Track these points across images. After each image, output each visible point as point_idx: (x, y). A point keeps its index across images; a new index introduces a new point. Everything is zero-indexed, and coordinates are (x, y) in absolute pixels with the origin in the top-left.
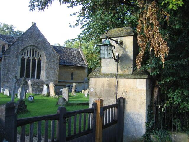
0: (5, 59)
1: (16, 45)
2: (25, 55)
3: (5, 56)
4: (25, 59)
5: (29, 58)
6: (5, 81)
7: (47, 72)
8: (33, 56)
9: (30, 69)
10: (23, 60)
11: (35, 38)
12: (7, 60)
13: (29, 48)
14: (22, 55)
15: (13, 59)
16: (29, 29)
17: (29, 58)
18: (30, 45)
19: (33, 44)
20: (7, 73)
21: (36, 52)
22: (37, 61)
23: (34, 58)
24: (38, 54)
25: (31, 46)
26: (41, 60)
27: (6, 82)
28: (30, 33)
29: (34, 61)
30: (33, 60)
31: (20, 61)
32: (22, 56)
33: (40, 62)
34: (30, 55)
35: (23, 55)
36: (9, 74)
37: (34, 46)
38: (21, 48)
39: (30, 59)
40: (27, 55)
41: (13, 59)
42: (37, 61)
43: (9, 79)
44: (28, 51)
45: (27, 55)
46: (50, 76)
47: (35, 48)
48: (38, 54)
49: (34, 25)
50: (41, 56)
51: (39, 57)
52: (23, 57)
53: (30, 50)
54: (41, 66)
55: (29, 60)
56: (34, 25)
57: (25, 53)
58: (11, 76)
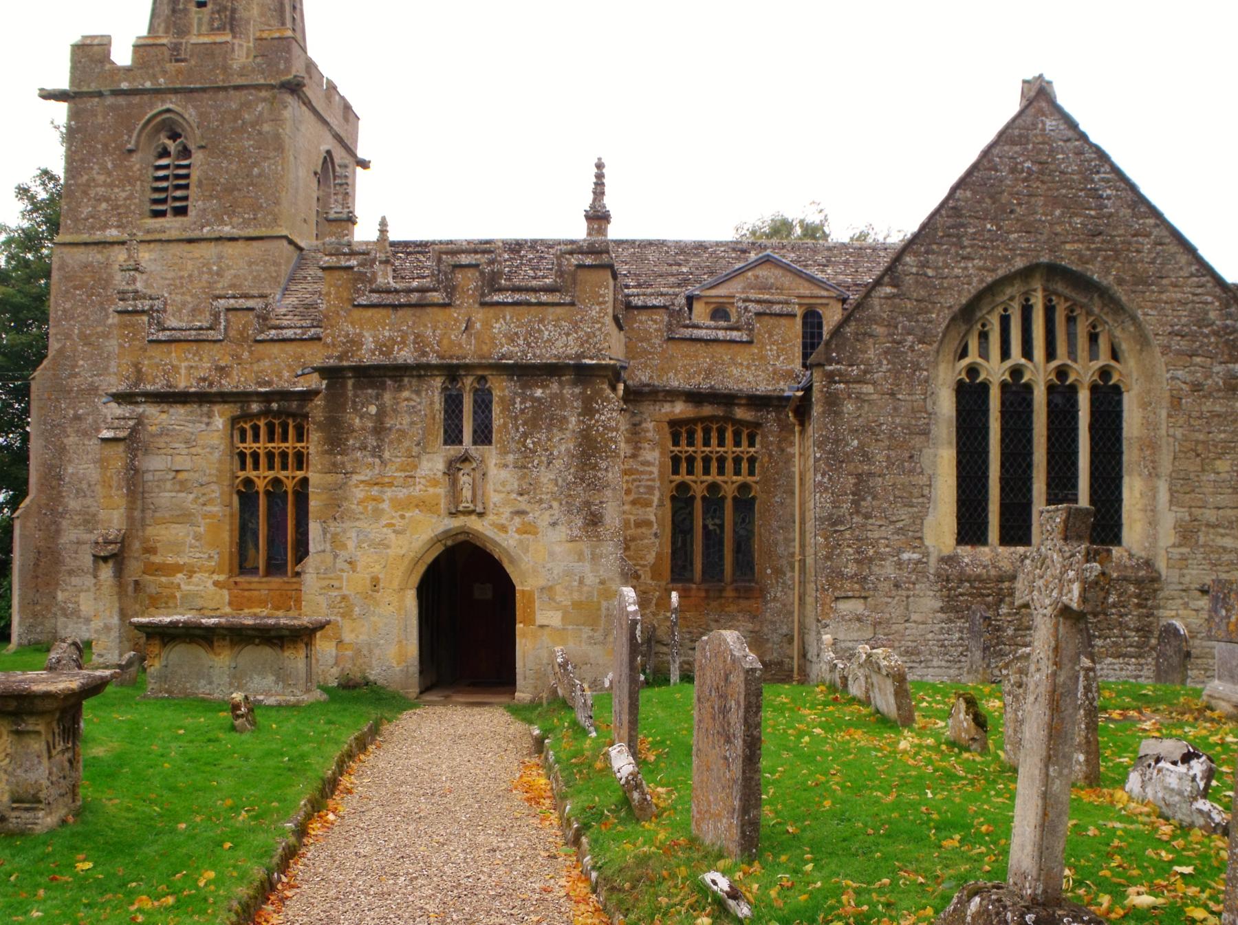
0: (832, 402)
1: (909, 280)
2: (984, 354)
3: (830, 378)
4: (985, 387)
5: (1016, 372)
6: (841, 575)
7: (1183, 487)
8: (1050, 354)
9: (1030, 466)
10: (971, 395)
11: (1055, 201)
12: (849, 407)
13: (1009, 291)
14: (964, 354)
15: (893, 394)
16: (1001, 134)
17: (1016, 372)
18: (1019, 263)
19: (1045, 259)
20: (858, 512)
21: (1071, 320)
22: (1084, 398)
23: (1062, 373)
24: (1093, 338)
25: (1026, 273)
26: (1117, 390)
27: (847, 585)
28: (1013, 170)
29: (1062, 395)
30: (1051, 389)
31: (946, 404)
32: (965, 362)
33: (1108, 399)
34: (1027, 352)
35: (973, 357)
36: (867, 516)
37: (1053, 271)
38: (956, 299)
39: (1028, 388)
40: (1005, 354)
41: (893, 394)
42: (1084, 398)
43: (871, 560)
44: (1005, 322)
45: (1005, 354)
46: (1210, 515)
47: (1060, 287)
48: (1093, 338)
49: (1039, 95)
50: (1115, 355)
51: (1104, 359)
52: (973, 371)
53: (1027, 312)
54: (1119, 439)
55: (1017, 394)
56: (1039, 95)
57: (984, 336)
58: (888, 531)
